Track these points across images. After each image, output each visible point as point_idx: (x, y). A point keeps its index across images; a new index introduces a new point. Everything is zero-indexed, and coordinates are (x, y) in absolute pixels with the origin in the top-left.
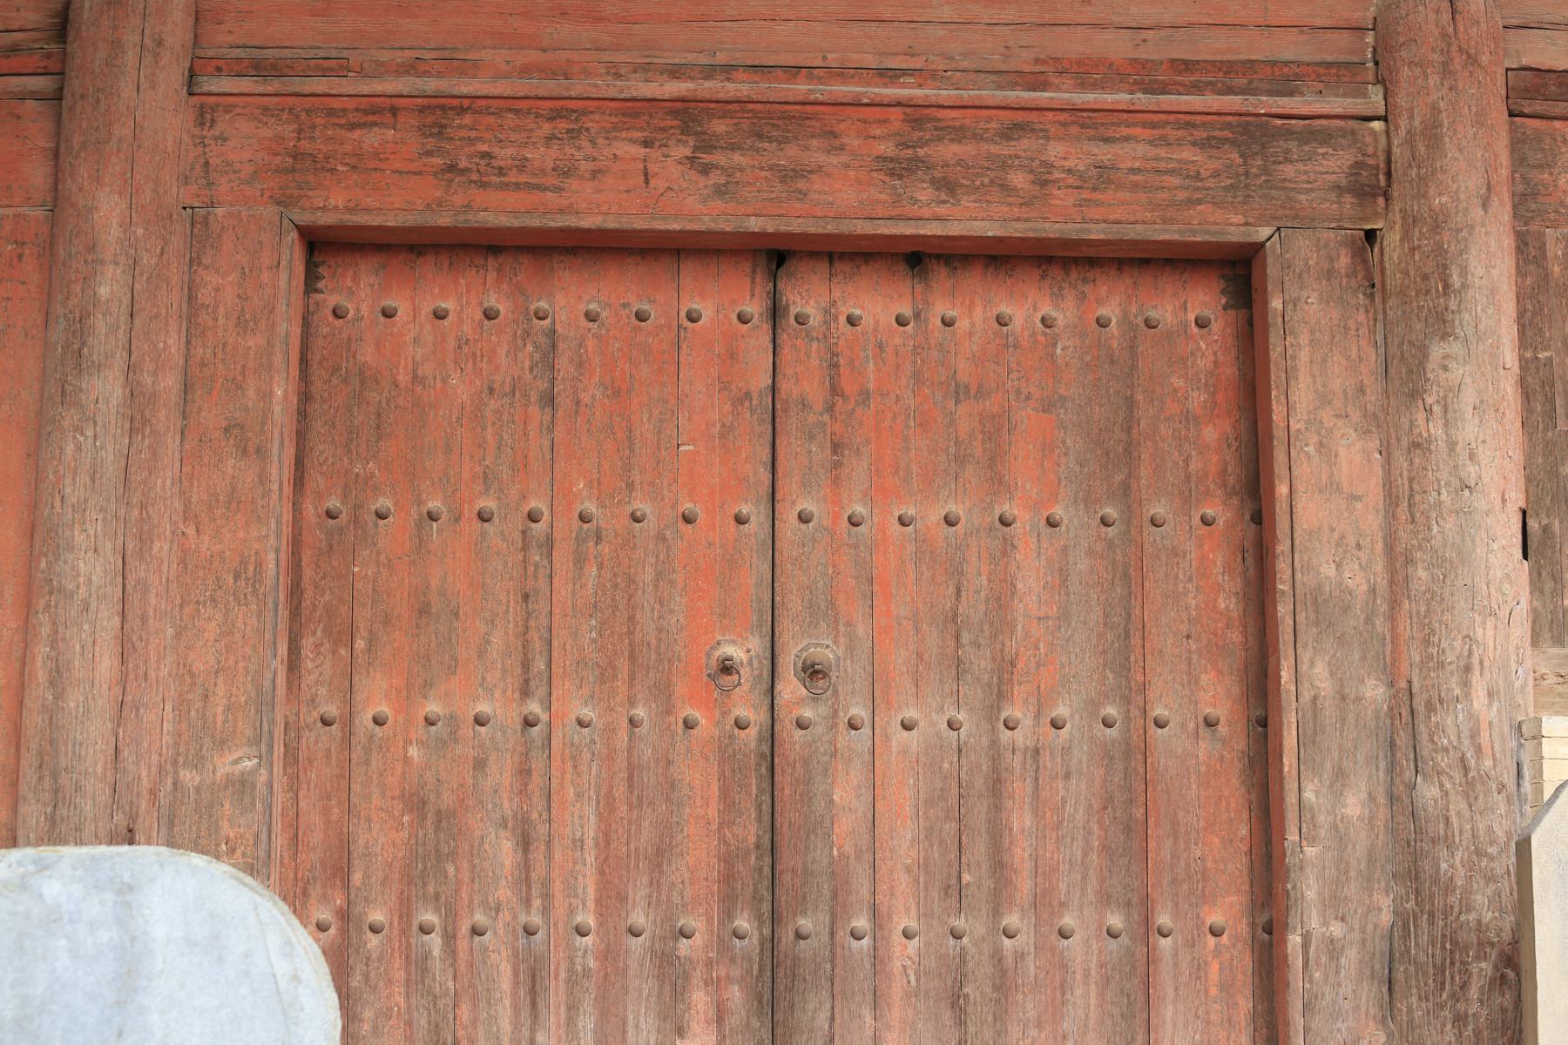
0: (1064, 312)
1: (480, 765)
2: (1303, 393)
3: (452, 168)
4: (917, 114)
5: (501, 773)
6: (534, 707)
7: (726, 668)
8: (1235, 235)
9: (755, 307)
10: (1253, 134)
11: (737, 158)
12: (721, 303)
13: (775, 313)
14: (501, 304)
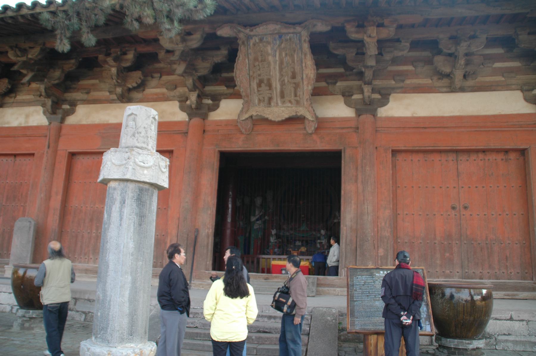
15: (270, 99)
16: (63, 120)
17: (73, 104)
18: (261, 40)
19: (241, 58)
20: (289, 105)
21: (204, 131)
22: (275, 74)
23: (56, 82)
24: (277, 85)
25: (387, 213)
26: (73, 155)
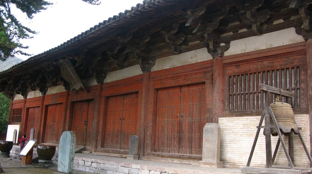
0: (197, 88)
1: (165, 124)
2: (207, 93)
3: (161, 84)
4: (185, 75)
5: (166, 124)
6: (168, 120)
7: (177, 116)
8: (203, 81)
9: (180, 90)
10: (205, 72)
11: (175, 80)
12: (178, 90)
13: (181, 91)
14: (167, 92)
15: (75, 82)
16: (45, 94)
17: (47, 88)
18: (64, 64)
19: (62, 71)
20: (80, 83)
21: (69, 95)
22: (72, 74)
23: (38, 82)
24: (74, 78)
25: (101, 123)
26: (47, 106)
